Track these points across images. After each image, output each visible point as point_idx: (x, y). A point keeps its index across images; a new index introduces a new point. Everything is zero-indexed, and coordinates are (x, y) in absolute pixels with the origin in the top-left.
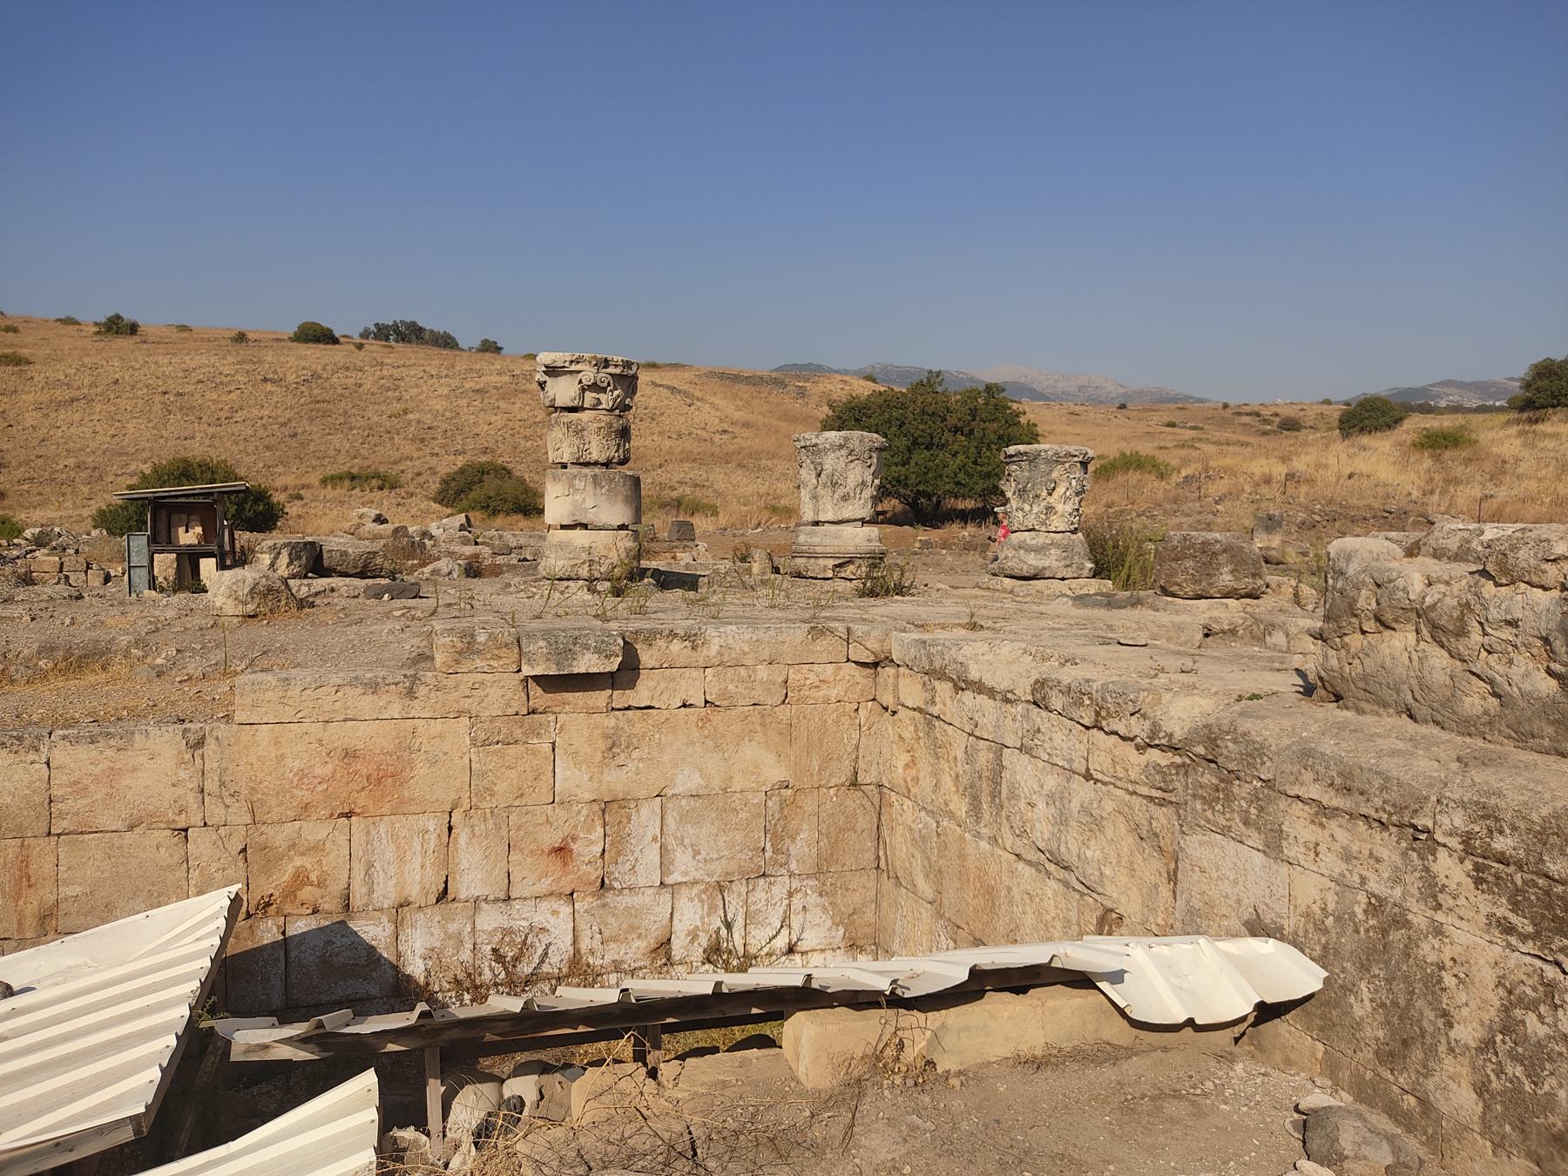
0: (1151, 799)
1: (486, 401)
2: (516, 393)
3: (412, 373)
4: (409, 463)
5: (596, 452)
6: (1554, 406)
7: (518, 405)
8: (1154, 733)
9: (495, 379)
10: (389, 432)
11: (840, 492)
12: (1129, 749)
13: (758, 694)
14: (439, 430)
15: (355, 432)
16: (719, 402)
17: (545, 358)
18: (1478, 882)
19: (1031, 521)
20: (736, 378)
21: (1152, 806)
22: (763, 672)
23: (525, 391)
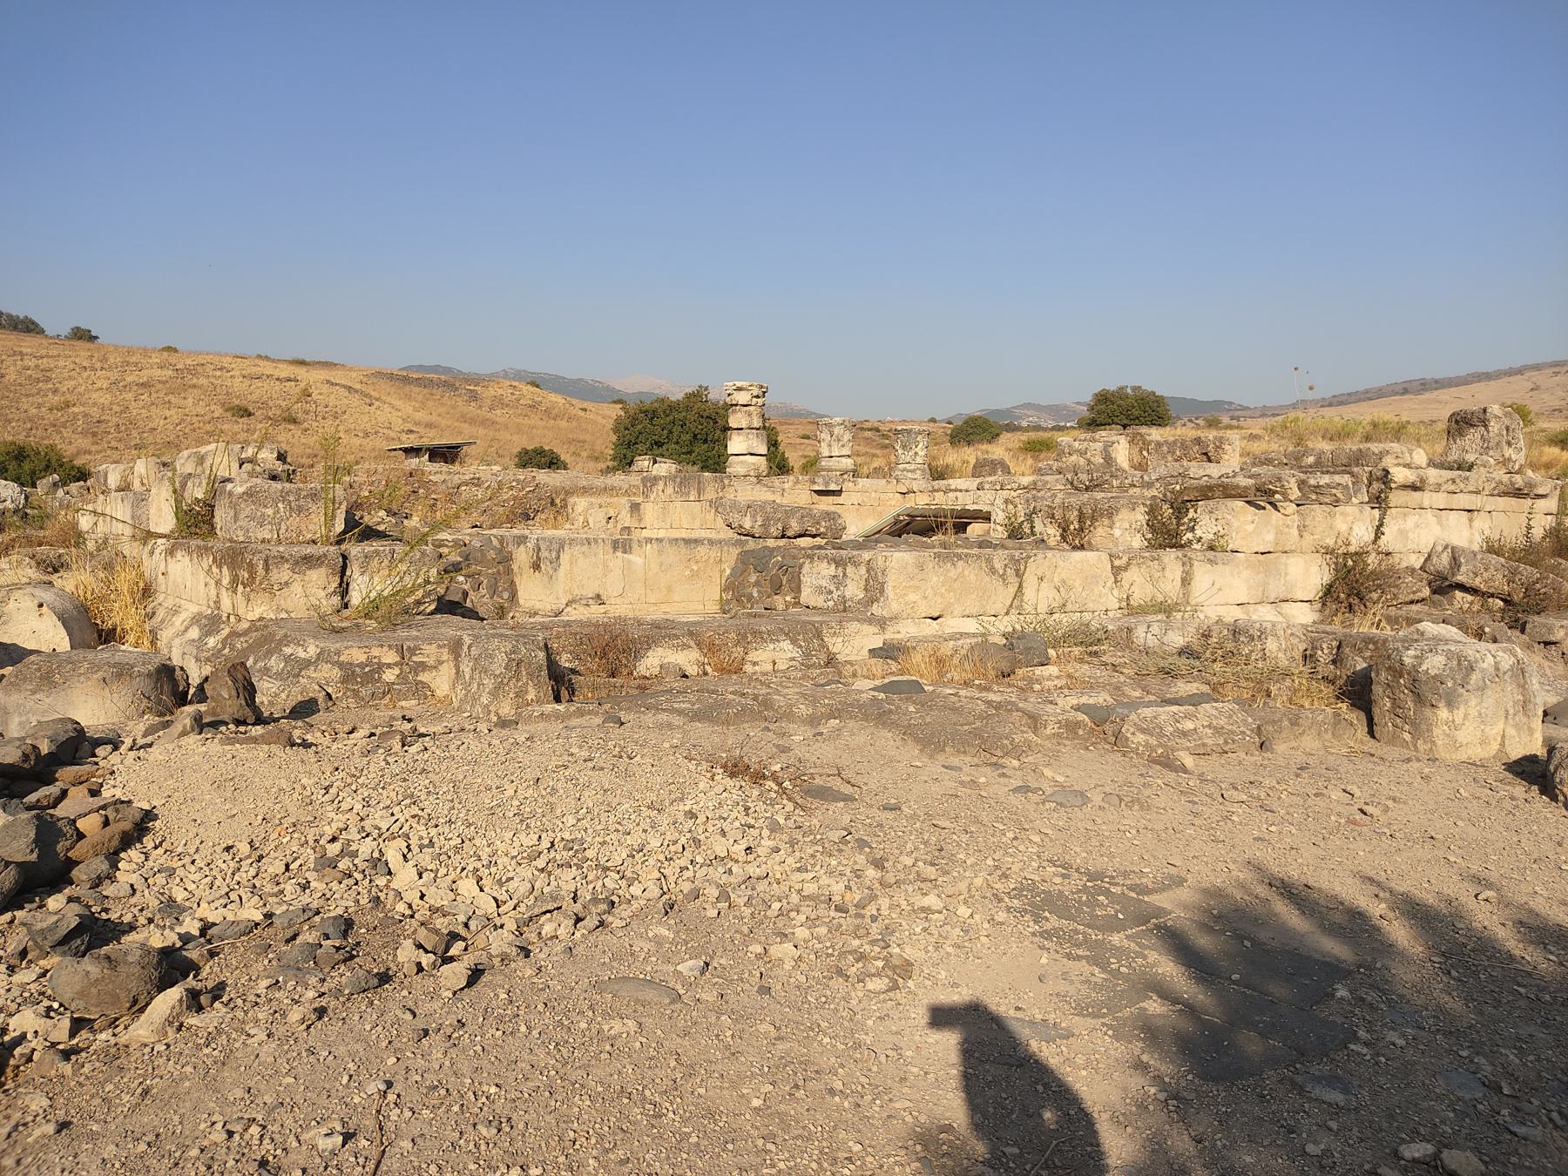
1: (154, 395)
2: (185, 388)
3: (61, 363)
4: (88, 457)
5: (756, 425)
6: (1109, 424)
7: (190, 400)
9: (157, 373)
10: (55, 426)
11: (841, 443)
13: (872, 502)
14: (110, 424)
15: (14, 424)
16: (398, 403)
17: (739, 384)
19: (907, 460)
20: (406, 380)
22: (873, 495)
23: (194, 386)
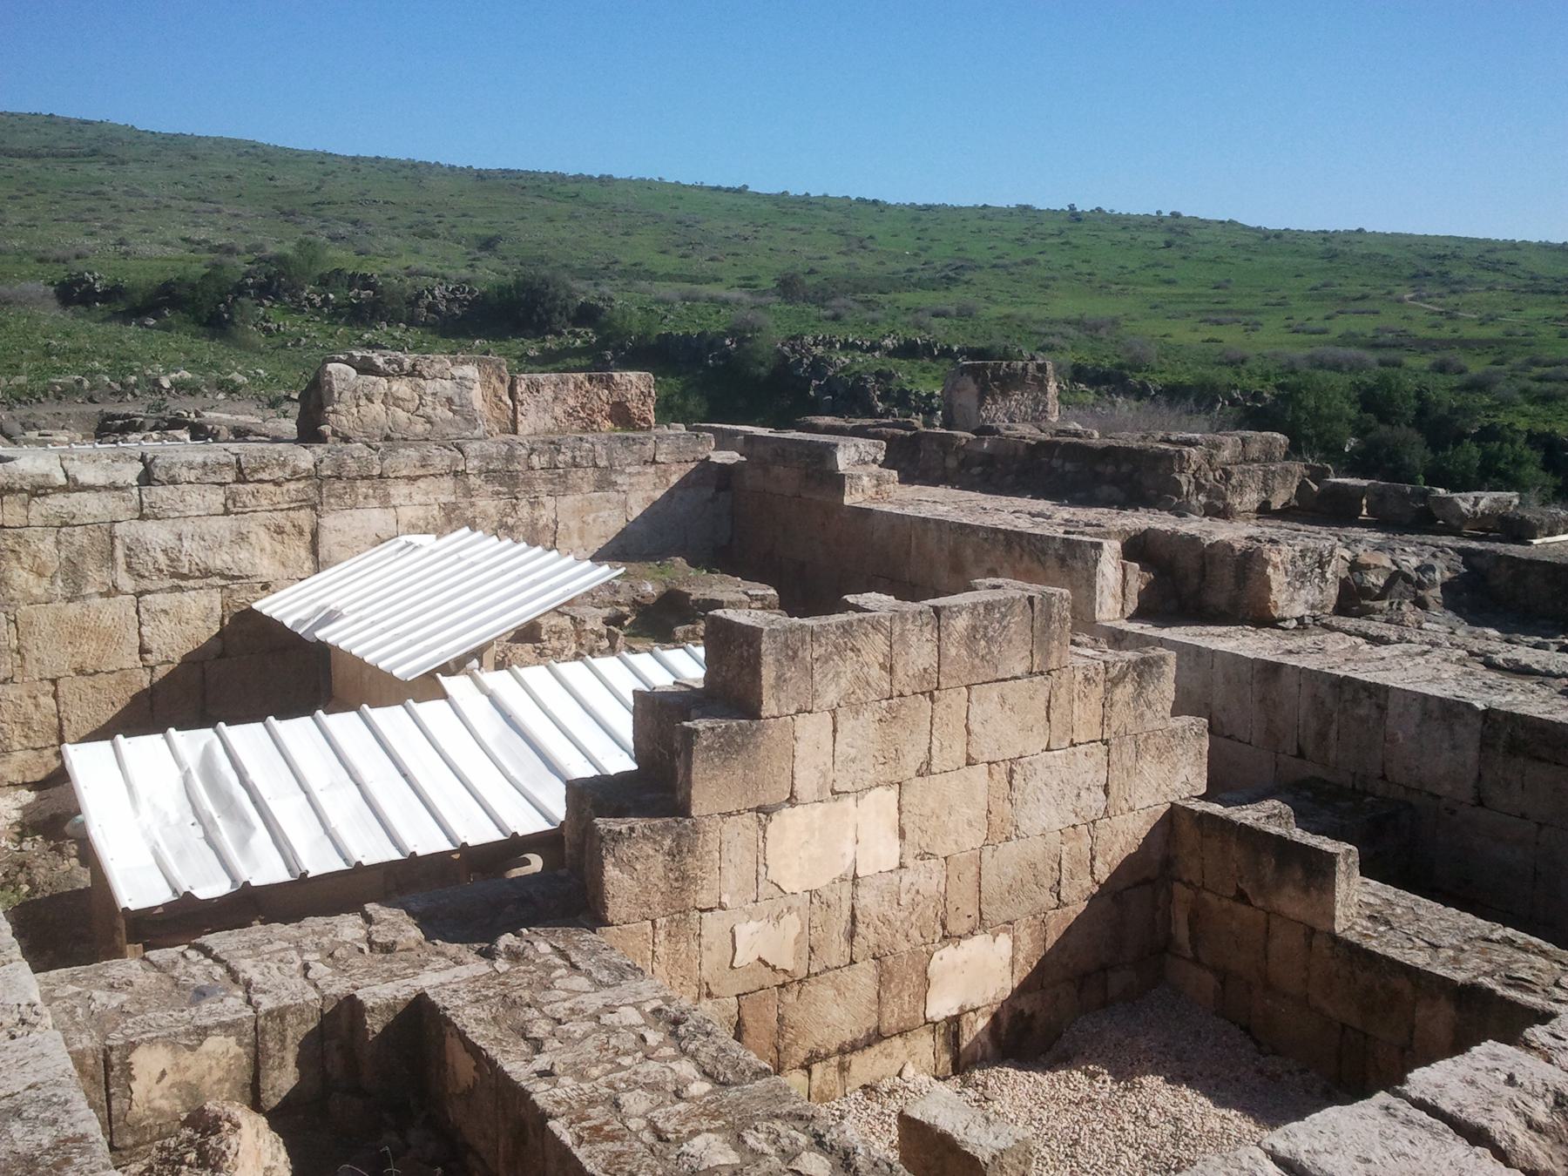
0: (289, 509)
8: (295, 473)
12: (270, 487)
18: (487, 482)
21: (291, 513)
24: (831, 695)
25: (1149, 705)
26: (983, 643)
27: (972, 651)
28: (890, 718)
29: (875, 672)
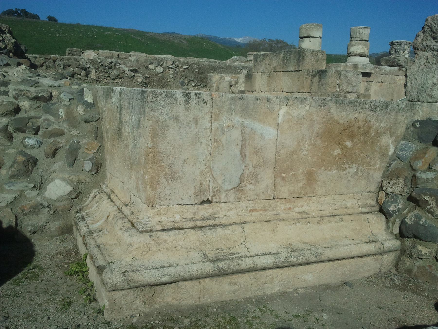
24: (261, 70)
25: (322, 85)
26: (286, 61)
27: (283, 63)
28: (269, 77)
29: (268, 66)
